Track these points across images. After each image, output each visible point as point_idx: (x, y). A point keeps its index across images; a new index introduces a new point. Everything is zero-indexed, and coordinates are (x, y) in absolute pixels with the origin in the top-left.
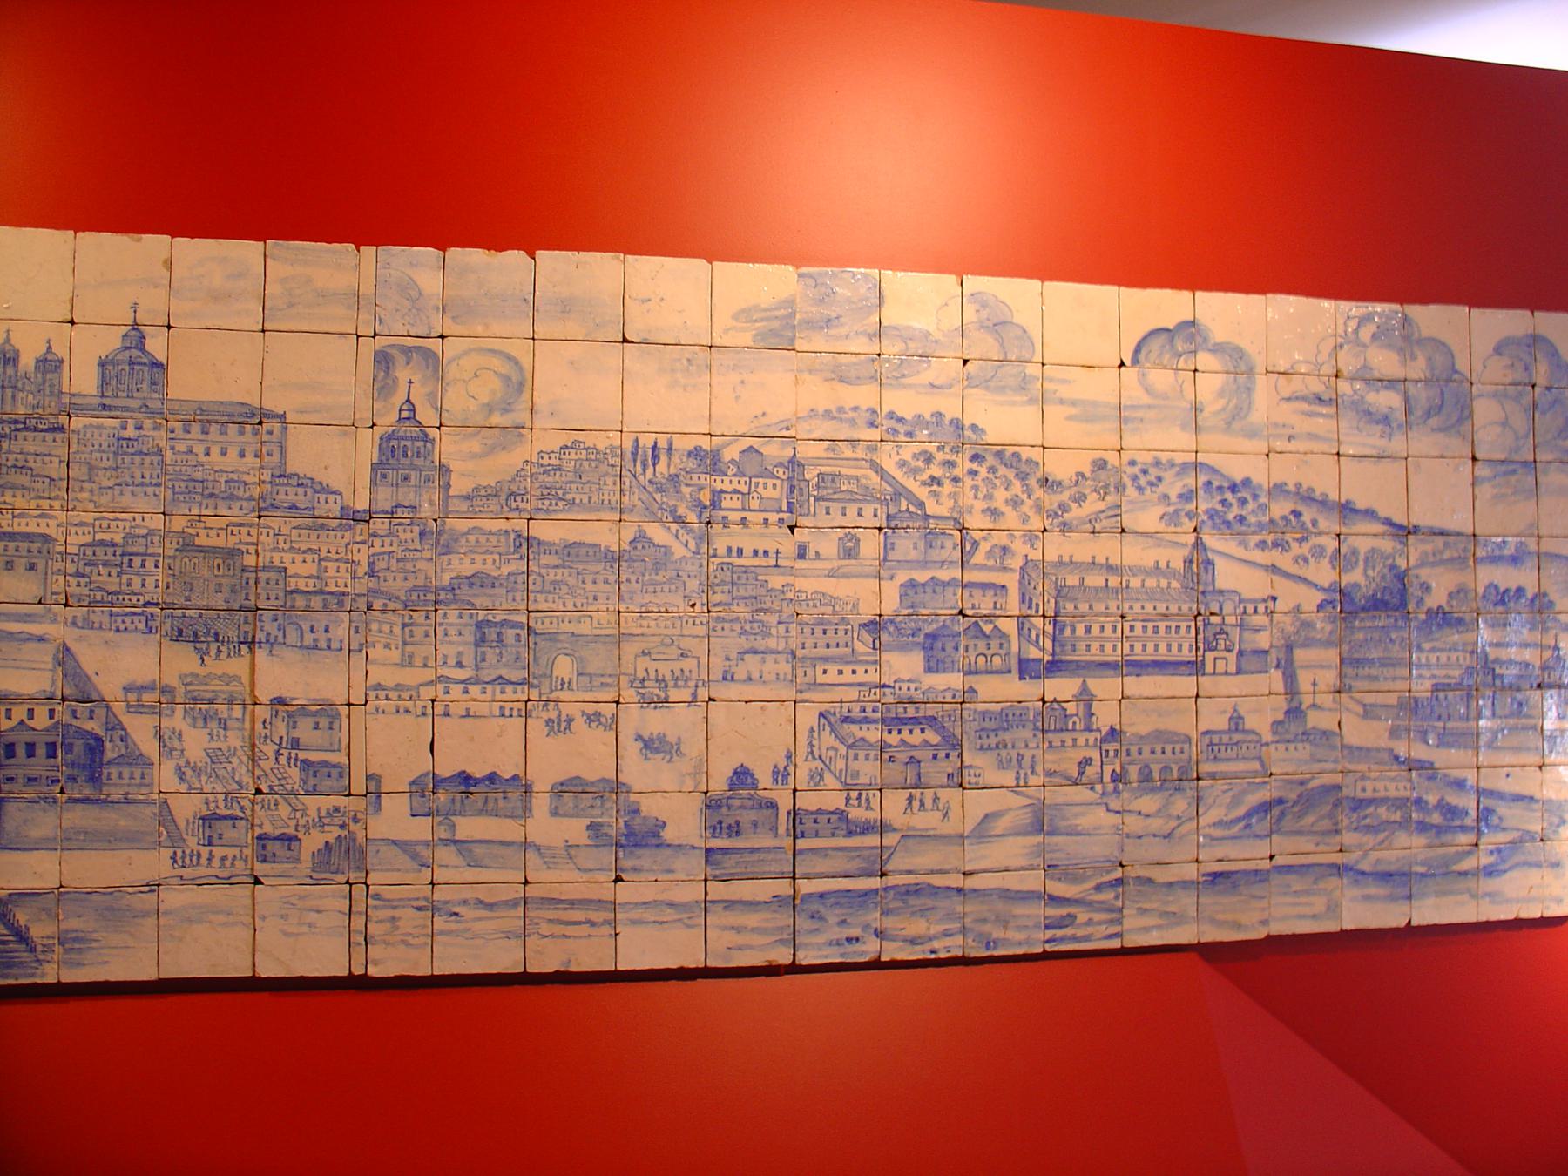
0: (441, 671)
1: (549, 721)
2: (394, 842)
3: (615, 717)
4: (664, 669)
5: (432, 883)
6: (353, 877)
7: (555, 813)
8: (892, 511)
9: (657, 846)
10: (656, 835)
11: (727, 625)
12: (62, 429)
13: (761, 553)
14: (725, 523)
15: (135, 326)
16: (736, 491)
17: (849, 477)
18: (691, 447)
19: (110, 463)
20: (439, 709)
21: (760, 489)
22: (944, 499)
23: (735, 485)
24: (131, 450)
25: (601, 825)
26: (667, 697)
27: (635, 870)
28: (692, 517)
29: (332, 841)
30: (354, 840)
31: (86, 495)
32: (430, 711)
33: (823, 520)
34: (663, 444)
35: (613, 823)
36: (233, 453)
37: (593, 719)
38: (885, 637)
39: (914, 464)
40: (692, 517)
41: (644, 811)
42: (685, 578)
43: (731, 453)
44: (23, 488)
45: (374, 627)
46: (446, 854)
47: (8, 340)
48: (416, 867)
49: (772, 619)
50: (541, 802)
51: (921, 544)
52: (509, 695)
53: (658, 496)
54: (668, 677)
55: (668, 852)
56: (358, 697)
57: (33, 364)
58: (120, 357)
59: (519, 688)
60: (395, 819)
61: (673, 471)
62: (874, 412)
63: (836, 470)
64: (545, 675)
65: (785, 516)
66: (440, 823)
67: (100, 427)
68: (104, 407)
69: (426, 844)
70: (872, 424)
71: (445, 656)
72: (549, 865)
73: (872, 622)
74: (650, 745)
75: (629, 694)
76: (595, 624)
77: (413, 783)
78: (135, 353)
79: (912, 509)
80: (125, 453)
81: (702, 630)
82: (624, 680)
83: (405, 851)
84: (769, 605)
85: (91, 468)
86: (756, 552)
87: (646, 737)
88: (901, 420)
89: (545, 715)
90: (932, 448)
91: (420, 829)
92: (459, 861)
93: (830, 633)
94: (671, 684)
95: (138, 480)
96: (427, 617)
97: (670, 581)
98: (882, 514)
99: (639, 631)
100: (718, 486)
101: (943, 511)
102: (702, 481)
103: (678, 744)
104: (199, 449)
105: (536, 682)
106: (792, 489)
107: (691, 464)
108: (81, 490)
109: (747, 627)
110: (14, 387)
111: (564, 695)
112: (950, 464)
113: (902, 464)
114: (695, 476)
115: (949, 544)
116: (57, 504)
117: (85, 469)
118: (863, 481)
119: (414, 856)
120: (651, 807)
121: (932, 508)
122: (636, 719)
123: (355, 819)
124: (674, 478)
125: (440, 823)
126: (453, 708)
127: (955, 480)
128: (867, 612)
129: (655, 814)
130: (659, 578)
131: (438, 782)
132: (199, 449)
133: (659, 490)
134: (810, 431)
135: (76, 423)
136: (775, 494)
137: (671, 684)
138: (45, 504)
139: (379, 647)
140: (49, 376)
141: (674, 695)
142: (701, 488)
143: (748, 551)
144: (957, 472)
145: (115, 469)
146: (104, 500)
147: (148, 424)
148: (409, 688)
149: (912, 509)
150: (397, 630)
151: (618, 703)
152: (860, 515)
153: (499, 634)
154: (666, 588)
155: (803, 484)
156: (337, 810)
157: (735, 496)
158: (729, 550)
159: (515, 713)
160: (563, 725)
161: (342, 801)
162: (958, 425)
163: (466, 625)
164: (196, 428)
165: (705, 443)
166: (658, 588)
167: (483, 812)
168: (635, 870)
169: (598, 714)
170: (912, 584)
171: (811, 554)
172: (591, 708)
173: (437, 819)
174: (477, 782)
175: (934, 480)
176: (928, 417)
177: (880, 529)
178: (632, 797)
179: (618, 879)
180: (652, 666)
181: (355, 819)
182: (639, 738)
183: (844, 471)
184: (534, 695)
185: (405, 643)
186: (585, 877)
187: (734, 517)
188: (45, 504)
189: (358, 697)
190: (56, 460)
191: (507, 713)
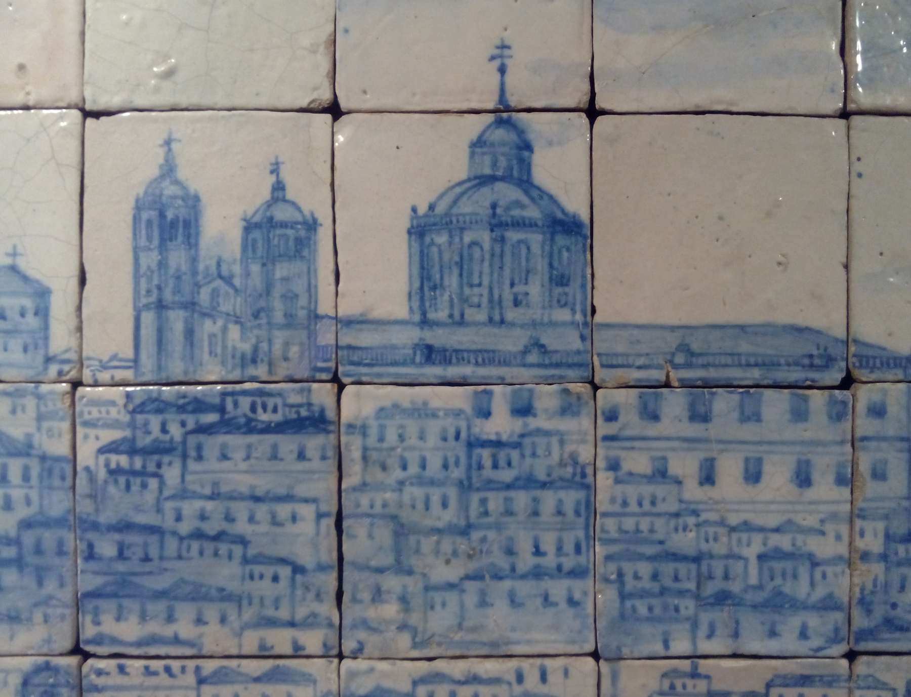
12: (317, 422)
15: (504, 112)
19: (448, 517)
24: (506, 475)
31: (390, 610)
36: (778, 475)
44: (224, 596)
47: (169, 169)
57: (235, 234)
58: (466, 207)
67: (422, 412)
68: (430, 353)
78: (507, 193)
80: (490, 485)
85: (401, 531)
95: (526, 561)
104: (685, 465)
108: (378, 595)
110: (190, 306)
116: (313, 641)
117: (384, 535)
132: (685, 465)
135: (358, 403)
138: (281, 640)
140: (281, 270)
145: (465, 531)
146: (440, 620)
147: (547, 397)
164: (674, 403)
188: (281, 640)
190: (307, 511)
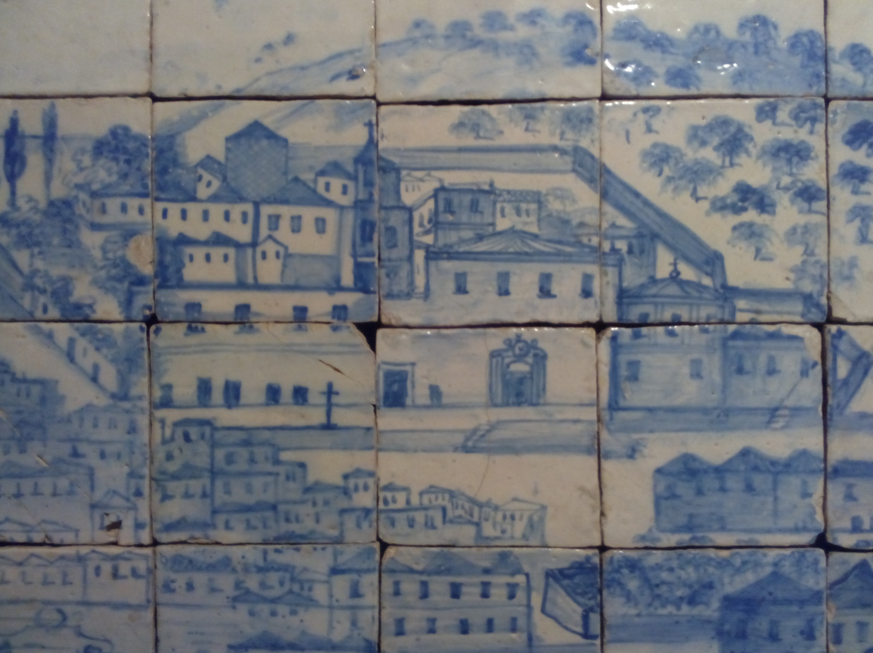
8: (633, 278)
11: (200, 579)
13: (287, 394)
14: (195, 320)
16: (219, 240)
17: (518, 197)
18: (101, 130)
21: (284, 233)
22: (775, 246)
23: (217, 224)
28: (108, 306)
33: (448, 308)
34: (32, 121)
38: (615, 607)
39: (692, 154)
40: (108, 306)
42: (93, 459)
43: (205, 140)
49: (314, 562)
51: (713, 367)
53: (22, 257)
61: (58, 191)
62: (582, 21)
63: (482, 178)
65: (349, 299)
70: (579, 56)
73: (581, 568)
79: (687, 273)
81: (134, 591)
84: (309, 524)
86: (273, 394)
88: (658, 43)
90: (742, 112)
93: (471, 594)
97: (57, 467)
98: (605, 287)
100: (174, 226)
101: (774, 275)
102: (133, 215)
106: (366, 230)
107: (103, 173)
109: (252, 583)
112: (791, 153)
113: (660, 157)
114: (113, 205)
115: (789, 362)
118: (555, 206)
121: (742, 269)
124: (61, 211)
127: (808, 194)
128: (569, 534)
130: (31, 459)
133: (27, 240)
134: (413, 80)
136: (324, 245)
142: (129, 234)
143: (253, 391)
144: (812, 172)
149: (687, 273)
152: (545, 292)
154: (46, 485)
155: (396, 219)
157: (217, 253)
158: (204, 388)
162: (814, 50)
165: (139, 118)
166: (27, 486)
170: (689, 469)
171: (419, 393)
175: (750, 197)
176: (730, 30)
177: (600, 327)
183: (504, 181)
187: (219, 303)
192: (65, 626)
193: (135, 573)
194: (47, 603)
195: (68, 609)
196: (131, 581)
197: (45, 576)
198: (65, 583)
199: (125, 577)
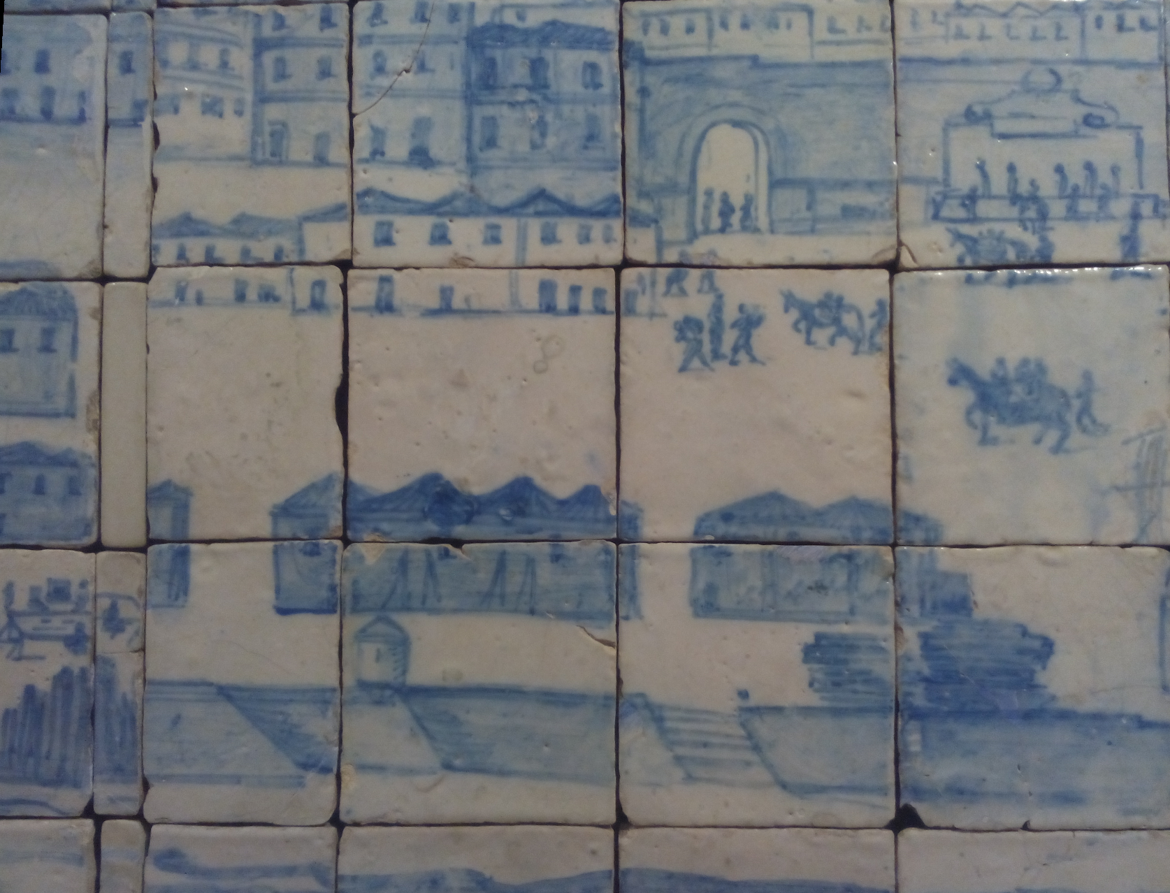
0: (368, 177)
1: (686, 327)
2: (226, 693)
3: (887, 315)
4: (1036, 165)
5: (336, 821)
6: (107, 794)
7: (706, 605)
9: (1029, 716)
10: (1028, 684)
20: (363, 290)
25: (848, 645)
26: (1046, 246)
27: (959, 792)
29: (44, 686)
30: (109, 683)
32: (333, 295)
35: (890, 642)
37: (820, 317)
41: (985, 605)
45: (177, 52)
46: (379, 733)
48: (289, 768)
50: (665, 573)
52: (569, 248)
54: (1048, 187)
55: (1061, 736)
56: (126, 256)
59: (597, 226)
60: (232, 623)
64: (671, 188)
66: (363, 635)
69: (320, 697)
71: (378, 134)
72: (693, 765)
74: (1002, 398)
75: (929, 241)
76: (821, 33)
77: (284, 511)
82: (913, 203)
83: (256, 721)
87: (984, 367)
89: (675, 309)
91: (302, 653)
92: (419, 753)
94: (1057, 208)
96: (326, 21)
99: (952, 49)
103: (1086, 394)
105: (645, 207)
111: (732, 247)
119: (285, 737)
120: (1006, 591)
122: (948, 318)
123: (114, 623)
125: (363, 635)
126: (406, 289)
129: (1021, 614)
131: (356, 510)
137: (1057, 208)
139: (190, 110)
141: (1068, 241)
148: (270, 227)
150: (241, 60)
151: (893, 267)
153: (537, 66)
156: (59, 591)
159: (586, 302)
160: (730, 337)
161: (72, 566)
163: (441, 40)
167: (491, 599)
168: (959, 792)
169: (834, 305)
172: (811, 286)
173: (355, 623)
174: (475, 507)
178: (946, 559)
179: (905, 819)
180: (998, 154)
181: (114, 623)
182: (961, 374)
184: (642, 246)
185: (263, 98)
186: (803, 810)
189: (126, 256)
191: (562, 301)
192: (1058, 91)
193: (1144, 24)
194: (1036, 62)
195: (1063, 70)
196: (1139, 34)
197: (1035, 30)
198: (1059, 38)
199: (1132, 29)
